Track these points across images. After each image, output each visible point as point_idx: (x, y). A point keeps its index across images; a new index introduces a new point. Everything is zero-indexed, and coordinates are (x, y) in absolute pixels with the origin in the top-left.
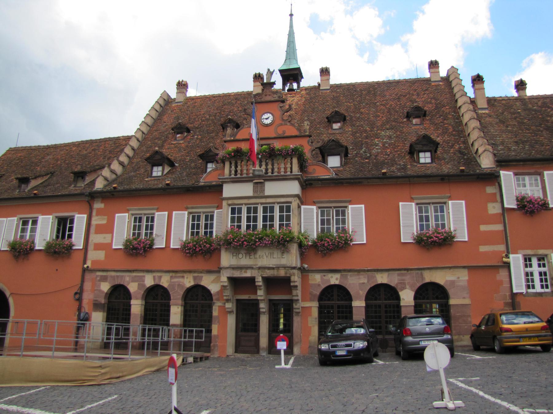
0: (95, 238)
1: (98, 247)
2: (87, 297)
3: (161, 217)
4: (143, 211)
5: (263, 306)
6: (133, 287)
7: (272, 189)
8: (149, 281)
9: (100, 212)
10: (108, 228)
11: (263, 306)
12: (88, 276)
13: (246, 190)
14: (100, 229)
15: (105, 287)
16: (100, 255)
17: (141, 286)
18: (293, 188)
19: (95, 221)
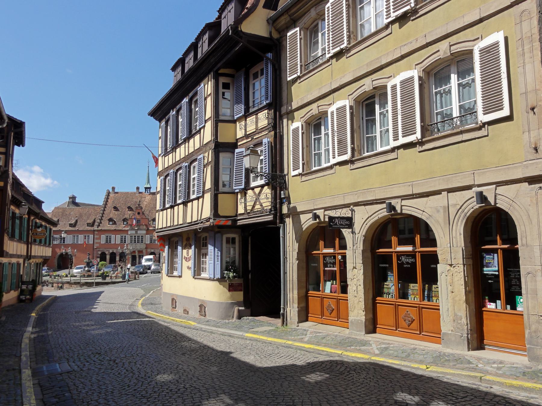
0: (96, 241)
1: (97, 243)
2: (95, 255)
3: (113, 236)
4: (109, 235)
5: (137, 256)
6: (107, 253)
7: (139, 232)
8: (111, 251)
9: (97, 234)
10: (100, 238)
11: (137, 256)
12: (95, 250)
13: (134, 232)
14: (97, 239)
15: (100, 253)
16: (98, 245)
17: (109, 252)
18: (144, 232)
19: (95, 237)
